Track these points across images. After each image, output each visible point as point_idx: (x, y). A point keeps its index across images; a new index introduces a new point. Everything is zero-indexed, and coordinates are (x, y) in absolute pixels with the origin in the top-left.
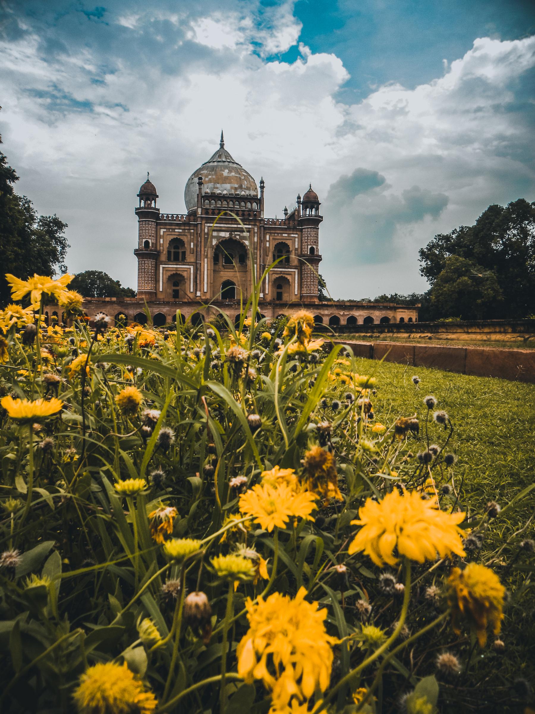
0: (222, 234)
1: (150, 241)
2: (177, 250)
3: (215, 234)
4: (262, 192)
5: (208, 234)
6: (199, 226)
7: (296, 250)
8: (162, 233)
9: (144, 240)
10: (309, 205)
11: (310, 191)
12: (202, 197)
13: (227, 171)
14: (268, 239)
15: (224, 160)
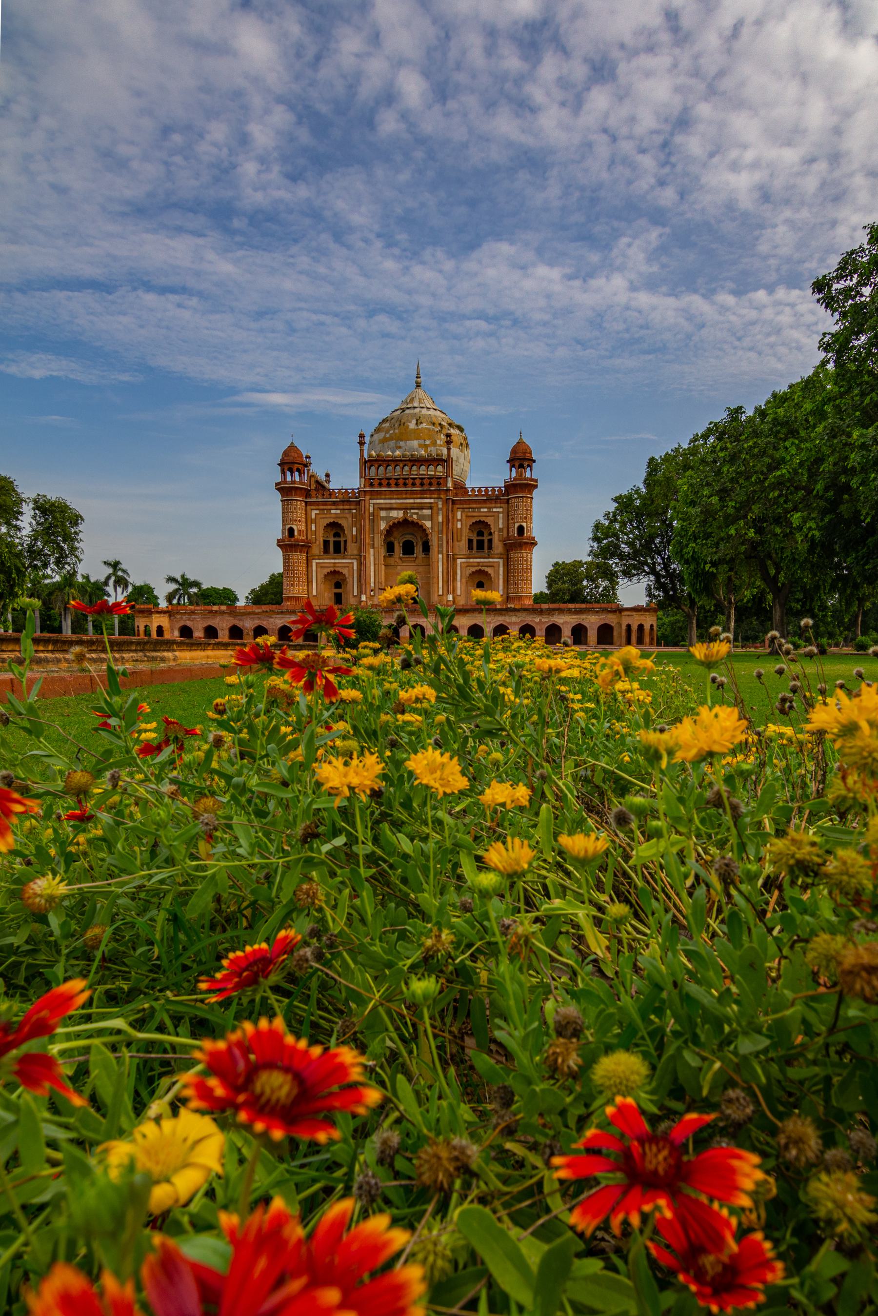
0: (394, 514)
1: (295, 527)
2: (337, 539)
3: (383, 513)
4: (449, 449)
5: (373, 514)
6: (362, 503)
7: (500, 530)
8: (313, 516)
9: (287, 527)
10: (517, 465)
11: (520, 443)
12: (366, 462)
13: (414, 421)
14: (459, 517)
15: (416, 405)
